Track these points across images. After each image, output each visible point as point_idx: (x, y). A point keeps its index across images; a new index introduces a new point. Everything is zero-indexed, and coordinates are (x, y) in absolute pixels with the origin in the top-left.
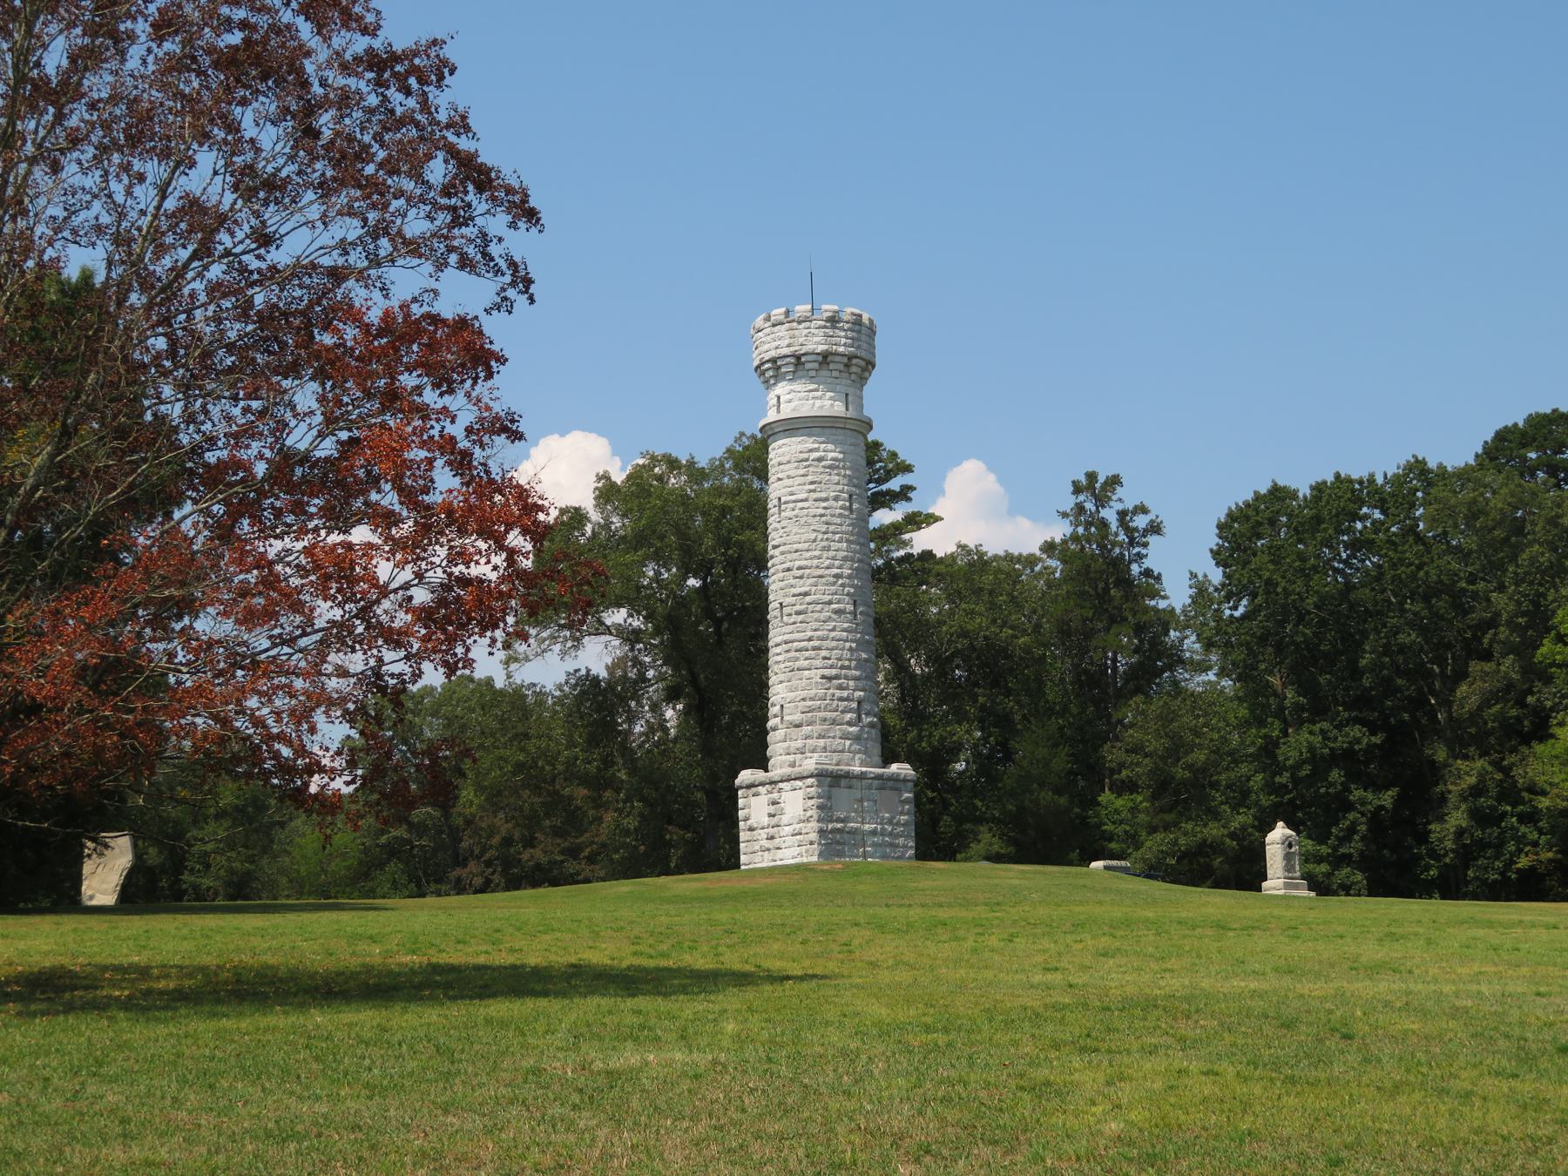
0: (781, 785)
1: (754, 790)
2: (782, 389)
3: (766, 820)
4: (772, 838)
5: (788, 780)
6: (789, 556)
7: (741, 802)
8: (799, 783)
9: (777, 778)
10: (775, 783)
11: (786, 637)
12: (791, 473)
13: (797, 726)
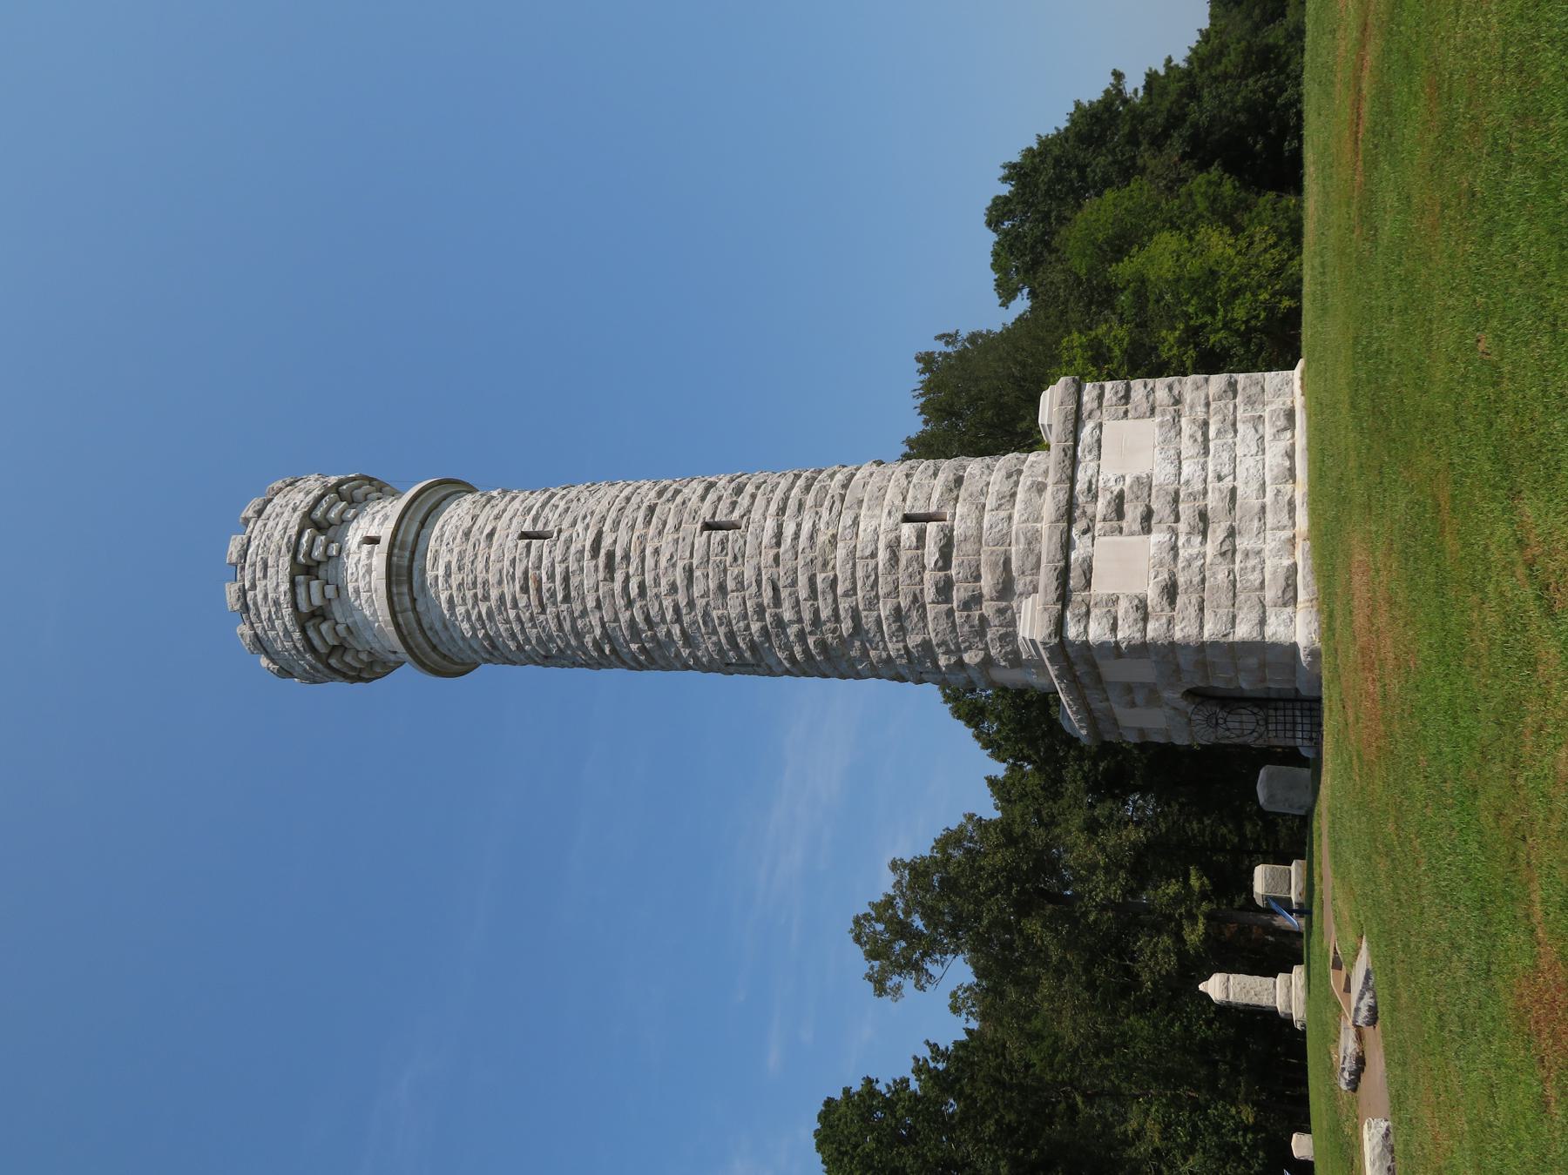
0: (1081, 486)
1: (1075, 580)
2: (354, 536)
3: (1158, 537)
4: (1203, 516)
5: (1075, 462)
6: (628, 511)
7: (1097, 632)
8: (1086, 433)
9: (1063, 497)
10: (1071, 503)
11: (773, 508)
12: (496, 511)
13: (959, 481)
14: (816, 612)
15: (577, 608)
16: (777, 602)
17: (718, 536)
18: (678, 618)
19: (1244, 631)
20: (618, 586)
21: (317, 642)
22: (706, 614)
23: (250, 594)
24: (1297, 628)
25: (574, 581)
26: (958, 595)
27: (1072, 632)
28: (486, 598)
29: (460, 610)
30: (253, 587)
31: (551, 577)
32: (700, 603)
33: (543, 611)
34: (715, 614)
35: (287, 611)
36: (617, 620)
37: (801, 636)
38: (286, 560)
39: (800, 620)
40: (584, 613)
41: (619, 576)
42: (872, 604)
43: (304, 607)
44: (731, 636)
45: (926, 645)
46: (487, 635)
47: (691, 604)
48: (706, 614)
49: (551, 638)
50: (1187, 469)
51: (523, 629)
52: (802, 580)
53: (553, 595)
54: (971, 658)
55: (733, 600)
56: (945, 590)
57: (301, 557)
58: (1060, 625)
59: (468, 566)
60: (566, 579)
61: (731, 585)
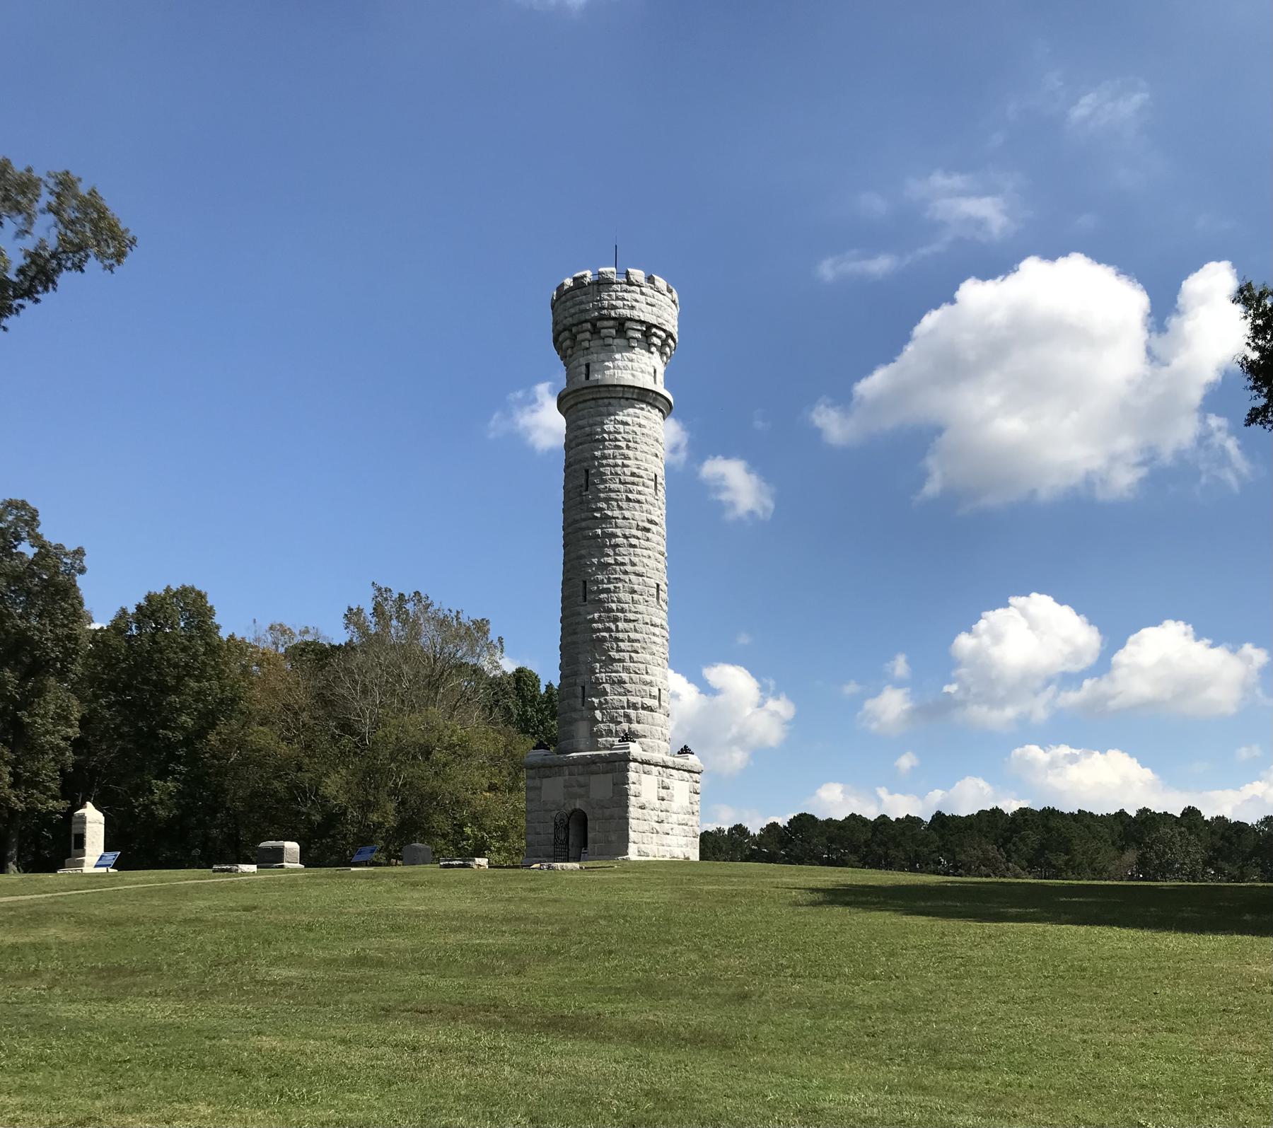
8: (686, 774)
9: (670, 764)
14: (622, 641)
15: (624, 505)
16: (627, 621)
17: (654, 591)
18: (617, 563)
19: (632, 835)
20: (634, 532)
21: (606, 323)
22: (619, 580)
23: (637, 289)
24: (633, 854)
25: (637, 505)
26: (632, 712)
27: (632, 764)
28: (628, 447)
29: (621, 428)
30: (642, 293)
31: (639, 493)
32: (626, 578)
33: (621, 482)
34: (620, 585)
35: (627, 313)
36: (617, 527)
37: (609, 630)
38: (655, 322)
39: (617, 631)
40: (620, 508)
41: (639, 534)
42: (626, 670)
43: (628, 324)
44: (608, 591)
45: (605, 693)
46: (604, 440)
47: (626, 573)
48: (619, 580)
49: (605, 482)
50: (675, 816)
51: (608, 465)
52: (637, 636)
53: (631, 492)
54: (598, 714)
55: (626, 597)
56: (634, 706)
57: (654, 330)
58: (635, 760)
59: (644, 439)
60: (639, 502)
61: (636, 597)
